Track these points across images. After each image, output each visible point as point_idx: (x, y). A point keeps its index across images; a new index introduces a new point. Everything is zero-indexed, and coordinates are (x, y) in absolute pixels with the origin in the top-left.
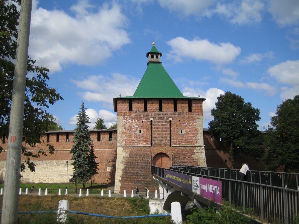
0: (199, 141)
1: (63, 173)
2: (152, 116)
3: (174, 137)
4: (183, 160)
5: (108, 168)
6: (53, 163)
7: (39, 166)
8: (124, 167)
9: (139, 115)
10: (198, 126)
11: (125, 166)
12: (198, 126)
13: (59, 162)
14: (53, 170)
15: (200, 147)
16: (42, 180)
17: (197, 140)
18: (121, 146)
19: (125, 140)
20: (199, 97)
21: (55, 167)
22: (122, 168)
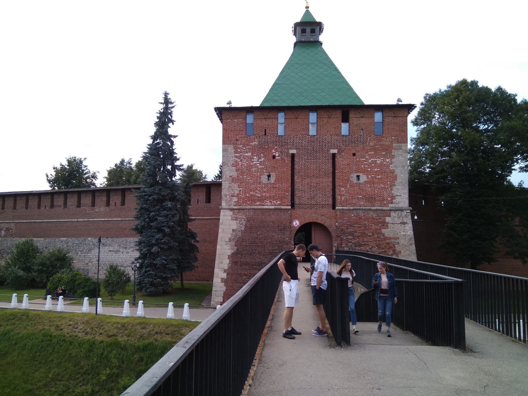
0: (398, 199)
2: (293, 144)
3: (341, 190)
4: (361, 240)
7: (107, 248)
8: (233, 251)
9: (267, 143)
10: (396, 167)
11: (236, 248)
12: (396, 167)
14: (129, 254)
15: (399, 212)
17: (393, 198)
18: (228, 207)
19: (238, 195)
20: (400, 103)
22: (229, 252)
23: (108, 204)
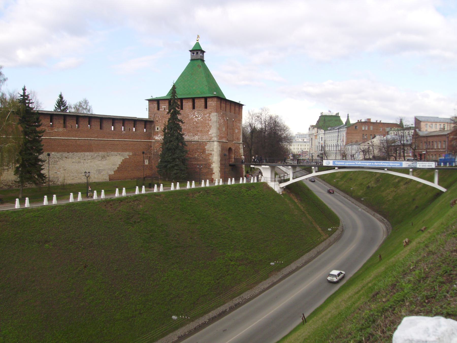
1: (101, 168)
5: (145, 160)
6: (87, 156)
7: (70, 160)
13: (94, 155)
16: (76, 177)
20: (240, 103)
21: (90, 160)
23: (65, 126)
